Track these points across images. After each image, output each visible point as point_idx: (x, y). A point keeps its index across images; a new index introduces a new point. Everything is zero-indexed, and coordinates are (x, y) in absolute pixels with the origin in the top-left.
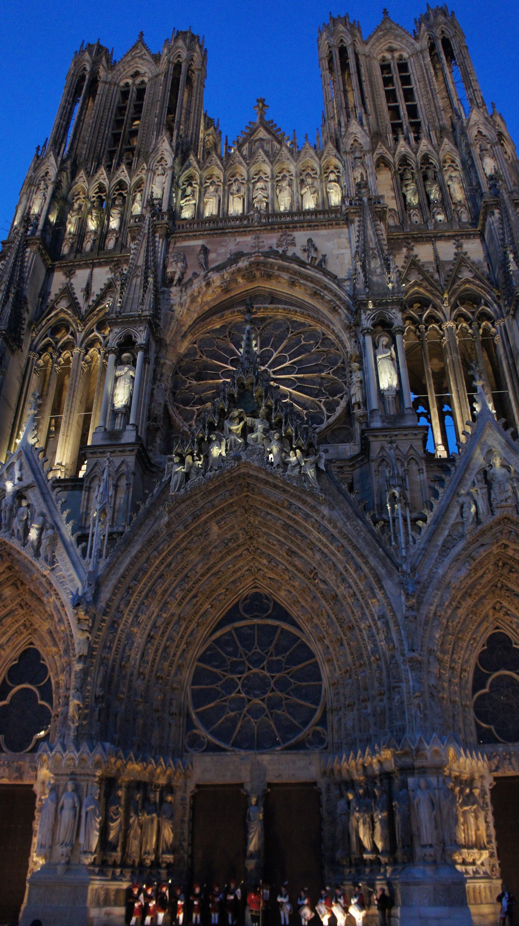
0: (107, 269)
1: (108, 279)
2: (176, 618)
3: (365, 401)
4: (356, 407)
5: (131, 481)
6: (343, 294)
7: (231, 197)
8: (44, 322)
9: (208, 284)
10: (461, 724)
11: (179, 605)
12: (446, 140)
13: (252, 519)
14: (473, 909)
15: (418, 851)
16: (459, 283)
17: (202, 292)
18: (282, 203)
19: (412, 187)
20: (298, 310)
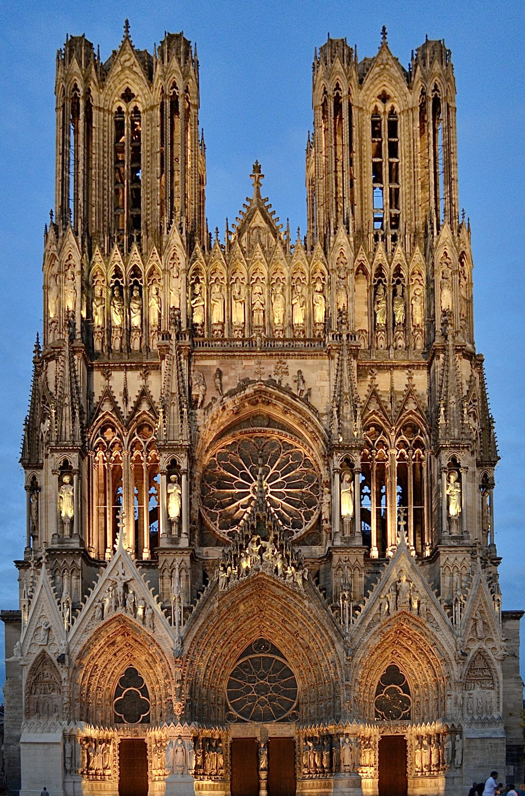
0: (138, 373)
2: (220, 655)
3: (331, 519)
4: (325, 521)
5: (189, 574)
6: (321, 428)
7: (234, 302)
8: (95, 424)
9: (224, 409)
10: (368, 712)
11: (222, 648)
12: (417, 248)
13: (263, 601)
14: (364, 790)
15: (343, 768)
16: (404, 414)
17: (220, 415)
18: (276, 314)
19: (383, 305)
20: (288, 434)
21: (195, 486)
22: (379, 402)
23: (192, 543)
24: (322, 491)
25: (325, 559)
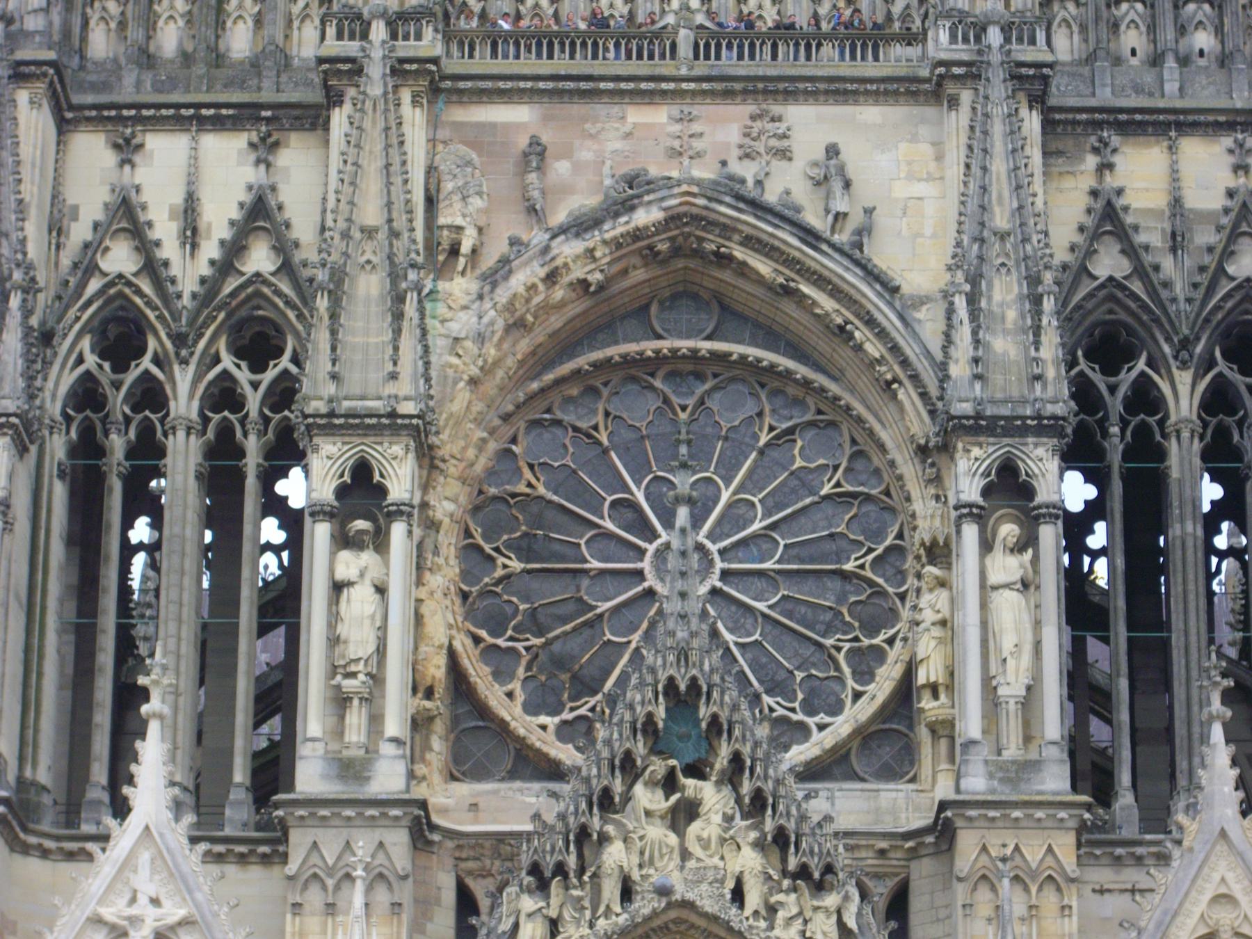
1: (250, 188)
4: (927, 695)
21: (436, 552)
22: (1130, 251)
23: (420, 769)
24: (919, 576)
25: (930, 839)
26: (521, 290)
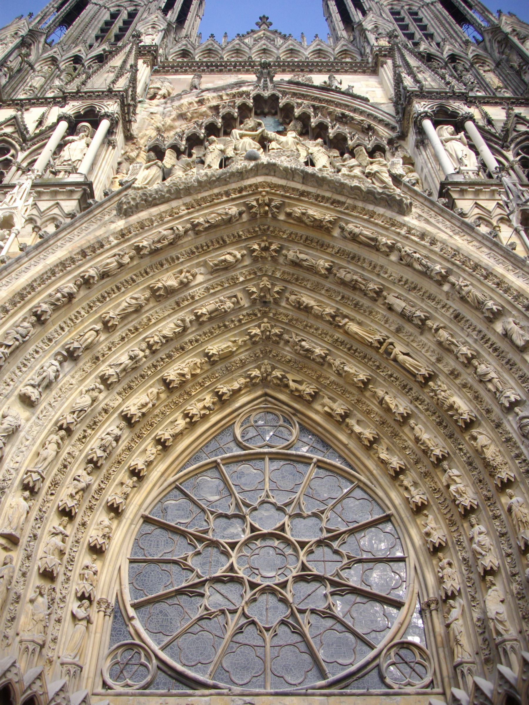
26: (186, 103)
